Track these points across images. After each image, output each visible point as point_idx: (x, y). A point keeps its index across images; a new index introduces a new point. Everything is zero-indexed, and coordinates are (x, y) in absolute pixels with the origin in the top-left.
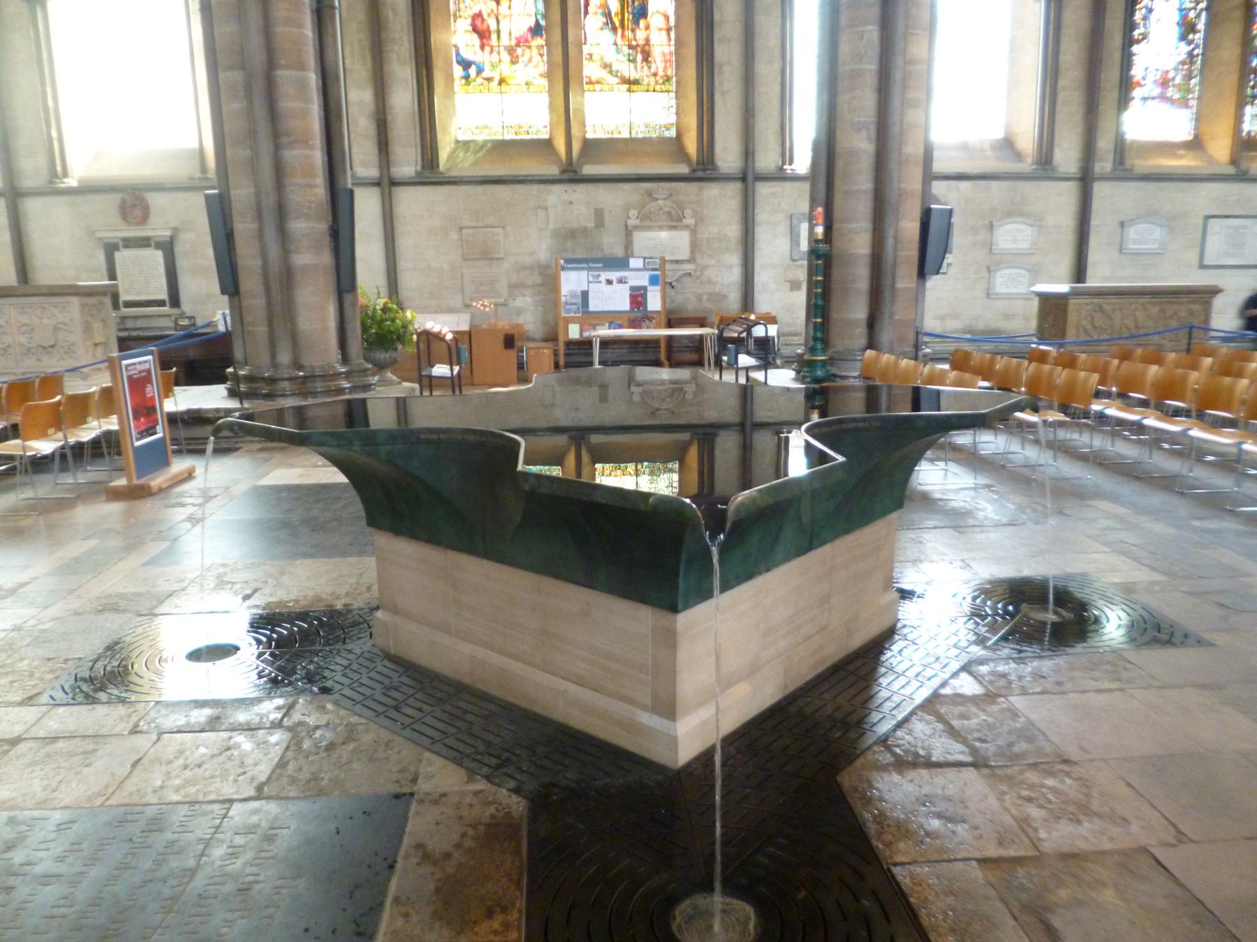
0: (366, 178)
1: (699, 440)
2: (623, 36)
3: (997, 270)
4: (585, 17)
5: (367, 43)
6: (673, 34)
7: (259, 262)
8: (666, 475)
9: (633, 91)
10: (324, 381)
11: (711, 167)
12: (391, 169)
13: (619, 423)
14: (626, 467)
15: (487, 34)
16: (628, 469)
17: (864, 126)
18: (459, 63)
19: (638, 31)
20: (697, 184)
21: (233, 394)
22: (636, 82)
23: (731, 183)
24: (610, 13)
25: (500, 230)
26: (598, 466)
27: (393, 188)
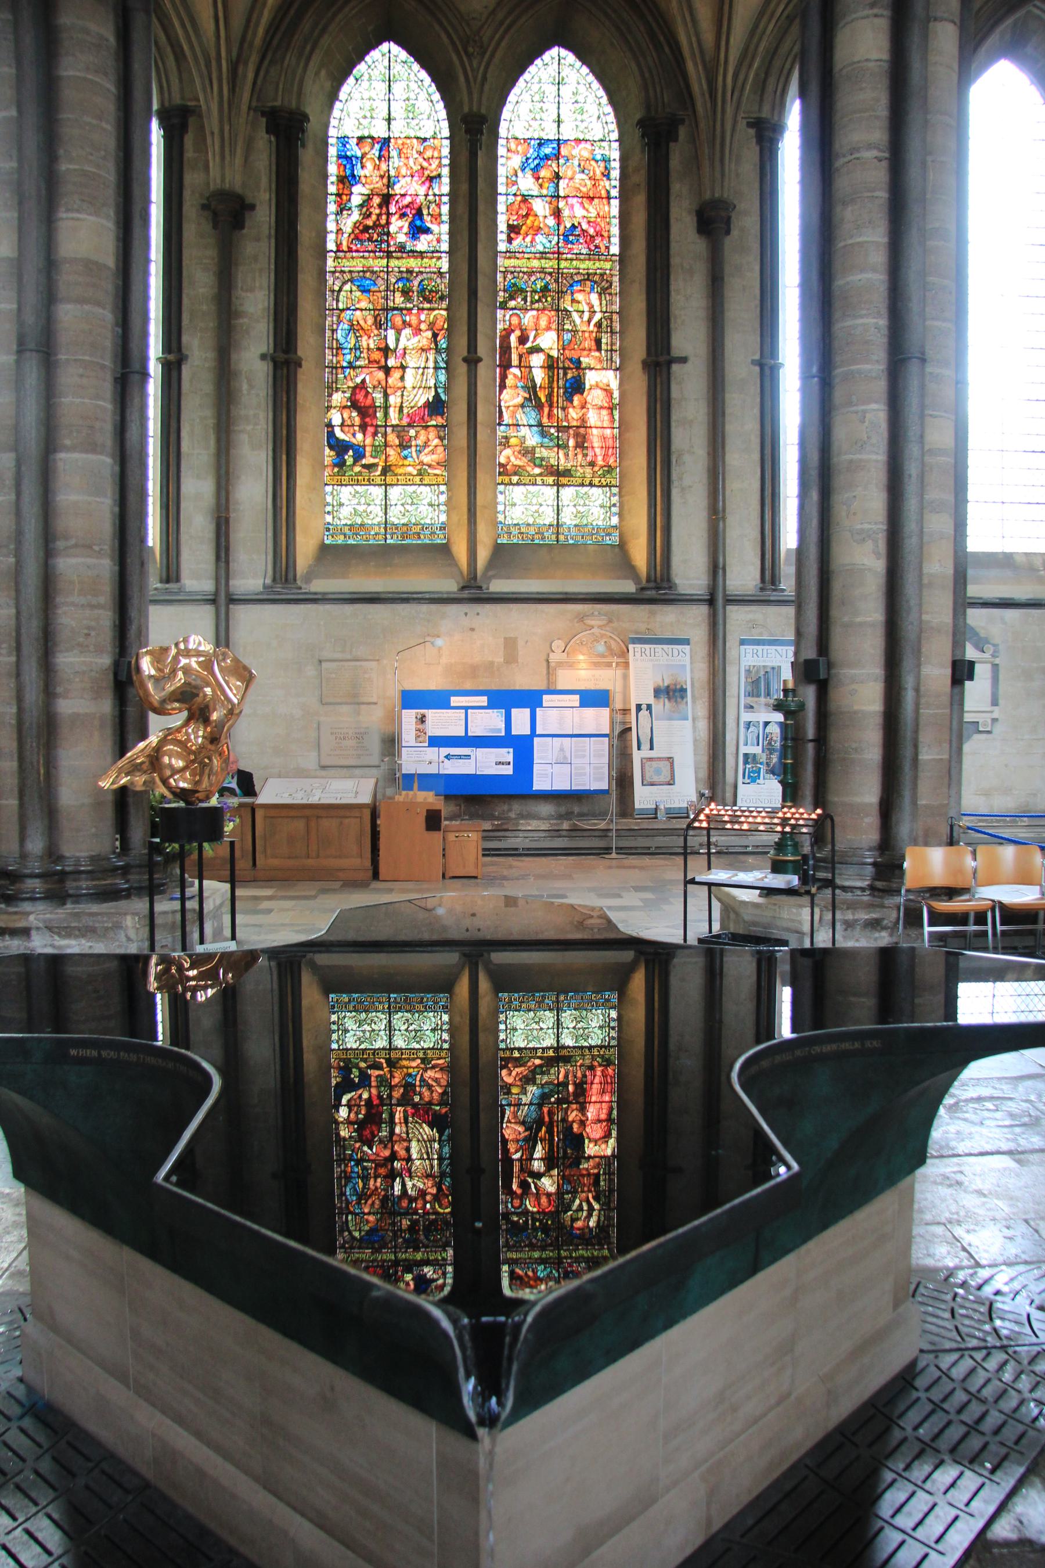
0: (196, 593)
2: (550, 416)
4: (501, 393)
5: (211, 422)
6: (616, 414)
7: (14, 710)
8: (599, 1011)
9: (564, 485)
11: (665, 585)
12: (231, 582)
13: (534, 937)
14: (544, 997)
15: (371, 411)
16: (547, 1001)
17: (869, 536)
18: (331, 447)
19: (571, 410)
20: (648, 607)
22: (567, 473)
23: (694, 607)
24: (534, 386)
25: (374, 664)
26: (504, 996)
27: (231, 606)
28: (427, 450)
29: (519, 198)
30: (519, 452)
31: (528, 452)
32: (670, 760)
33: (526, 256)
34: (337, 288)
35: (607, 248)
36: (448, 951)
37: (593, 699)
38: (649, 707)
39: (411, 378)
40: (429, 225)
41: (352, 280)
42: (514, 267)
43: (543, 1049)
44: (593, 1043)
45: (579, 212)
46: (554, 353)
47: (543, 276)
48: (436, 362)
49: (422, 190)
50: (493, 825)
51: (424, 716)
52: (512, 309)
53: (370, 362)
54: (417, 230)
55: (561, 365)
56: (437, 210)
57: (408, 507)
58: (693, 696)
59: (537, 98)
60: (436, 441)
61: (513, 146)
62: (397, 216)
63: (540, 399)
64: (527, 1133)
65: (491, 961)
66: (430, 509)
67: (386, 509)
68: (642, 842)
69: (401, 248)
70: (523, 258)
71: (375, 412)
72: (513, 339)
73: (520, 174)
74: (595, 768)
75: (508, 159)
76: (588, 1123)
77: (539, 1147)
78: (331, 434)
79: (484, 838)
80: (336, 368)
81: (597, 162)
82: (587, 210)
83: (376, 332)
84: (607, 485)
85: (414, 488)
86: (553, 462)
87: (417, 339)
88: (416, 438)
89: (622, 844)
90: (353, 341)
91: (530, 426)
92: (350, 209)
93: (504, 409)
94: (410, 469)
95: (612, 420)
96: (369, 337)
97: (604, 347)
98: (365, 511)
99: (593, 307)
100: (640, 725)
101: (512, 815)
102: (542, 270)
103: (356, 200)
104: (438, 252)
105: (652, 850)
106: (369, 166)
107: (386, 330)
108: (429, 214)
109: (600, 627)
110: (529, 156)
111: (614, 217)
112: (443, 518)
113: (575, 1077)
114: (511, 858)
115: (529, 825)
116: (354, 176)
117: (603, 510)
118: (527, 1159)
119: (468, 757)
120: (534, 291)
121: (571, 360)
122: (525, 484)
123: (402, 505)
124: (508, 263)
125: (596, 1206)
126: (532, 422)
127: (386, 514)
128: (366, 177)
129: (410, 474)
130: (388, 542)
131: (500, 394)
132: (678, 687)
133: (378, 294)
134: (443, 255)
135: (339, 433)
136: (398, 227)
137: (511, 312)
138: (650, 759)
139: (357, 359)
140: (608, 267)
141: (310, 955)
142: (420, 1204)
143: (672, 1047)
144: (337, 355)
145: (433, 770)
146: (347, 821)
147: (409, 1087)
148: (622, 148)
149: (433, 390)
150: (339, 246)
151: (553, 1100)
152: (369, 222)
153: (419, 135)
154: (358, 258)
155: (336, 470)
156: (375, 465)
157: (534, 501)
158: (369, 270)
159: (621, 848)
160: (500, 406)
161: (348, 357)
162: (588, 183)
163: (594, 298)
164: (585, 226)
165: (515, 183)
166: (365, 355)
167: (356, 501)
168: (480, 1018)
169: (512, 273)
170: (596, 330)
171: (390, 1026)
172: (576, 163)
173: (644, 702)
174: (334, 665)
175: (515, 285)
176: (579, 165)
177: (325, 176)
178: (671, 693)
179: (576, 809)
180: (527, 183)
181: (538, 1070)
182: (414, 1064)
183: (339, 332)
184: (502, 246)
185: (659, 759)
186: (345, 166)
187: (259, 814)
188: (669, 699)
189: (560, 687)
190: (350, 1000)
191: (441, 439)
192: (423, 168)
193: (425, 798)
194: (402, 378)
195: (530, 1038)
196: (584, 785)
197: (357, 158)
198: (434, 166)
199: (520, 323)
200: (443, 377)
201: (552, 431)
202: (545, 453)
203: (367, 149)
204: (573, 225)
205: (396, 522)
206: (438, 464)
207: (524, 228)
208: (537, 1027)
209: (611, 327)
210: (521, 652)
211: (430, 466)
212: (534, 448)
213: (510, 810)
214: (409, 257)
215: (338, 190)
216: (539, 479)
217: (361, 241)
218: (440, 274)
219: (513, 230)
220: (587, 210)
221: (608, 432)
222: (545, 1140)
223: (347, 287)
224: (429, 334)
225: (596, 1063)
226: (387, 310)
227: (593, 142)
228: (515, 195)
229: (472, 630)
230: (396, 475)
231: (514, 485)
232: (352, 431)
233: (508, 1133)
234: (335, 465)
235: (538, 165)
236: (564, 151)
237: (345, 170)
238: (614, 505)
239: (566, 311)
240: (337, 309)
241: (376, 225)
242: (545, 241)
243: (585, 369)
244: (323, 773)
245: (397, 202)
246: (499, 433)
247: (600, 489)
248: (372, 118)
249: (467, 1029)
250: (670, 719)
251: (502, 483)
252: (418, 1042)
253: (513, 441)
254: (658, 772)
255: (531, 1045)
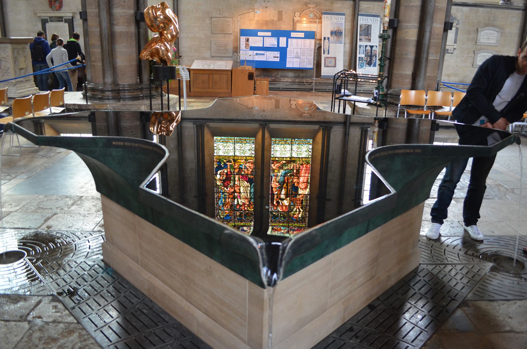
1: (323, 129)
3: (478, 54)
8: (306, 146)
10: (130, 92)
13: (284, 119)
14: (287, 140)
16: (288, 142)
21: (85, 97)
25: (230, 19)
32: (335, 58)
36: (255, 123)
37: (309, 35)
38: (328, 38)
43: (286, 158)
44: (303, 157)
50: (272, 79)
51: (248, 39)
58: (345, 35)
64: (279, 186)
65: (269, 127)
68: (324, 87)
74: (308, 60)
76: (300, 183)
77: (283, 190)
79: (270, 84)
89: (316, 88)
100: (325, 45)
101: (279, 76)
105: (327, 90)
109: (313, 8)
113: (297, 167)
114: (277, 91)
115: (285, 80)
118: (279, 194)
119: (264, 54)
125: (302, 210)
132: (339, 31)
138: (328, 58)
141: (207, 123)
142: (243, 207)
143: (330, 158)
145: (251, 58)
146: (222, 76)
147: (240, 169)
151: (289, 175)
159: (316, 89)
168: (265, 146)
171: (234, 148)
173: (327, 36)
174: (216, 19)
178: (337, 33)
179: (301, 75)
181: (284, 165)
182: (242, 161)
185: (331, 58)
187: (191, 72)
188: (336, 36)
189: (298, 29)
190: (221, 139)
193: (249, 68)
195: (282, 154)
196: (305, 66)
208: (284, 150)
210: (284, 16)
213: (278, 74)
222: (285, 188)
225: (303, 163)
229: (266, 7)
233: (273, 185)
244: (212, 59)
249: (260, 150)
250: (336, 43)
252: (244, 154)
254: (330, 62)
255: (282, 156)
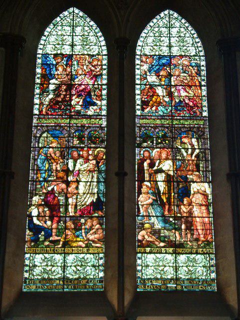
2: (170, 210)
4: (138, 197)
9: (179, 254)
18: (30, 230)
19: (182, 207)
22: (181, 245)
28: (91, 232)
29: (148, 86)
30: (150, 233)
31: (155, 232)
33: (153, 118)
34: (38, 135)
35: (201, 113)
39: (82, 188)
40: (95, 101)
41: (48, 131)
42: (146, 124)
45: (183, 94)
46: (171, 173)
47: (163, 129)
48: (98, 178)
49: (91, 82)
52: (144, 148)
53: (57, 178)
54: (88, 104)
55: (175, 180)
56: (100, 93)
57: (78, 268)
59: (157, 34)
60: (98, 226)
61: (144, 59)
62: (76, 96)
63: (163, 200)
66: (93, 269)
67: (64, 269)
69: (78, 113)
70: (151, 119)
71: (60, 208)
72: (146, 164)
73: (148, 74)
75: (141, 65)
78: (31, 221)
80: (36, 181)
81: (193, 67)
82: (188, 93)
83: (61, 160)
84: (207, 253)
85: (82, 256)
86: (171, 238)
87: (86, 165)
88: (85, 224)
90: (47, 166)
91: (157, 217)
92: (48, 92)
93: (140, 207)
94: (81, 243)
95: (209, 213)
96: (57, 164)
97: (201, 169)
98: (50, 270)
99: (194, 146)
102: (162, 126)
103: (52, 87)
104: (100, 115)
106: (60, 69)
107: (68, 159)
108: (95, 95)
110: (153, 64)
111: (204, 96)
112: (101, 274)
116: (51, 75)
117: (205, 270)
120: (158, 137)
121: (181, 177)
122: (154, 253)
123: (75, 266)
124: (141, 121)
126: (158, 214)
127: (64, 272)
128: (58, 75)
129: (81, 247)
130: (65, 290)
131: (138, 198)
133: (64, 139)
134: (103, 117)
135: (35, 221)
136: (77, 102)
137: (144, 150)
139: (49, 176)
140: (202, 123)
144: (37, 174)
148: (206, 60)
149: (96, 195)
150: (41, 112)
152: (60, 99)
153: (89, 53)
154: (52, 118)
155: (33, 244)
156: (59, 241)
157: (161, 264)
158: (59, 125)
160: (138, 205)
161: (44, 175)
162: (188, 78)
163: (194, 141)
164: (187, 101)
165: (146, 78)
166: (54, 174)
167: (45, 263)
169: (144, 127)
170: (196, 159)
172: (181, 67)
175: (146, 134)
176: (183, 69)
177: (35, 74)
180: (152, 79)
183: (39, 160)
184: (138, 113)
186: (46, 69)
191: (101, 224)
192: (92, 71)
194: (77, 188)
197: (53, 65)
198: (98, 70)
199: (150, 155)
200: (102, 187)
201: (171, 219)
202: (167, 233)
203: (59, 60)
204: (180, 100)
205: (71, 277)
206: (99, 240)
207: (151, 102)
209: (205, 158)
211: (94, 241)
212: (160, 230)
214: (83, 118)
215: (41, 81)
216: (163, 249)
217: (54, 110)
218: (102, 128)
219: (145, 104)
220: (188, 93)
221: (206, 219)
223: (45, 135)
224: (94, 162)
226: (69, 148)
227: (190, 57)
228: (145, 85)
230: (72, 247)
231: (148, 253)
232: (44, 219)
234: (32, 241)
235: (159, 68)
236: (174, 62)
237: (45, 71)
238: (212, 266)
239: (177, 148)
240: (38, 147)
241: (63, 100)
242: (163, 109)
243: (190, 182)
245: (76, 88)
246: (138, 221)
247: (203, 256)
248: (63, 44)
251: (140, 253)
253: (147, 226)
